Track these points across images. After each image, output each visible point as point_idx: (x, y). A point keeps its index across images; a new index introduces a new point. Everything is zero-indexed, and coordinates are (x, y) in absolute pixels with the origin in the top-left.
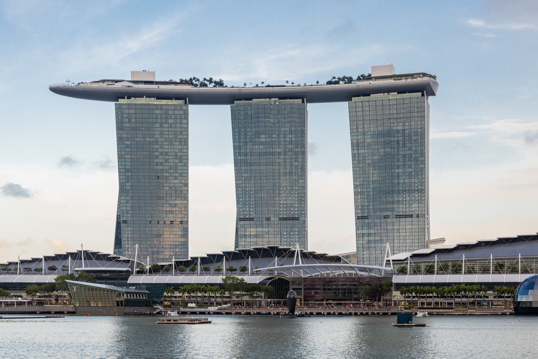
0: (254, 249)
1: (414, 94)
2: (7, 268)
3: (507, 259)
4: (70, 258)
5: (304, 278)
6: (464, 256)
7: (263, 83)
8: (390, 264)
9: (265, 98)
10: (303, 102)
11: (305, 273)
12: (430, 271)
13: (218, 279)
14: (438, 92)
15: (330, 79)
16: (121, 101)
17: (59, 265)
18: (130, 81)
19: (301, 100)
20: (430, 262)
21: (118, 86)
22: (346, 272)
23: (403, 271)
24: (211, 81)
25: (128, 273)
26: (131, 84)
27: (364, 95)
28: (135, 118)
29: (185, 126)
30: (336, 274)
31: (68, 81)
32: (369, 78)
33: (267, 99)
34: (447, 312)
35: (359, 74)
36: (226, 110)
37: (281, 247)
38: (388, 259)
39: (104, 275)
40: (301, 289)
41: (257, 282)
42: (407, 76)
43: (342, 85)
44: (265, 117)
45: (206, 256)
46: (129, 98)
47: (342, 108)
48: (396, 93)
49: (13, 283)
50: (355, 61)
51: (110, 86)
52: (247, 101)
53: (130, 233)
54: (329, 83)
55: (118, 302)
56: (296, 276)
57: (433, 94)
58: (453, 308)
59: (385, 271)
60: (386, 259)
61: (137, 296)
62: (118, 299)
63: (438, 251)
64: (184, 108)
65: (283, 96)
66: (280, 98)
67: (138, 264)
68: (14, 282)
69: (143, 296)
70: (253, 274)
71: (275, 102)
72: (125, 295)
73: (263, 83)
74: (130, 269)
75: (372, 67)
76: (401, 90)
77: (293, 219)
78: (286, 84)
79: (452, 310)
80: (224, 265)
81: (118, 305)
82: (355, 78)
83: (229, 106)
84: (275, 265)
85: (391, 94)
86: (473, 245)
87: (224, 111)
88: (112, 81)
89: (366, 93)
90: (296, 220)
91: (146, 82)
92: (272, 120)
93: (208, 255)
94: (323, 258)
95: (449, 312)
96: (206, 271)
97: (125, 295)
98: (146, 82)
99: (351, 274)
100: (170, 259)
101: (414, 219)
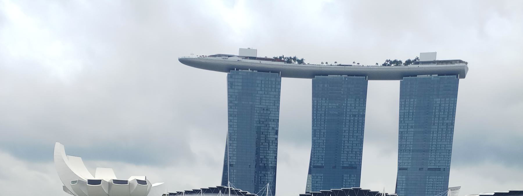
7: (336, 62)
9: (338, 75)
18: (238, 57)
24: (295, 59)
31: (192, 54)
33: (339, 76)
35: (407, 59)
47: (395, 85)
50: (405, 50)
52: (324, 77)
65: (350, 74)
71: (345, 78)
73: (336, 62)
78: (353, 65)
82: (404, 62)
83: (311, 80)
85: (433, 75)
87: (308, 83)
89: (414, 74)
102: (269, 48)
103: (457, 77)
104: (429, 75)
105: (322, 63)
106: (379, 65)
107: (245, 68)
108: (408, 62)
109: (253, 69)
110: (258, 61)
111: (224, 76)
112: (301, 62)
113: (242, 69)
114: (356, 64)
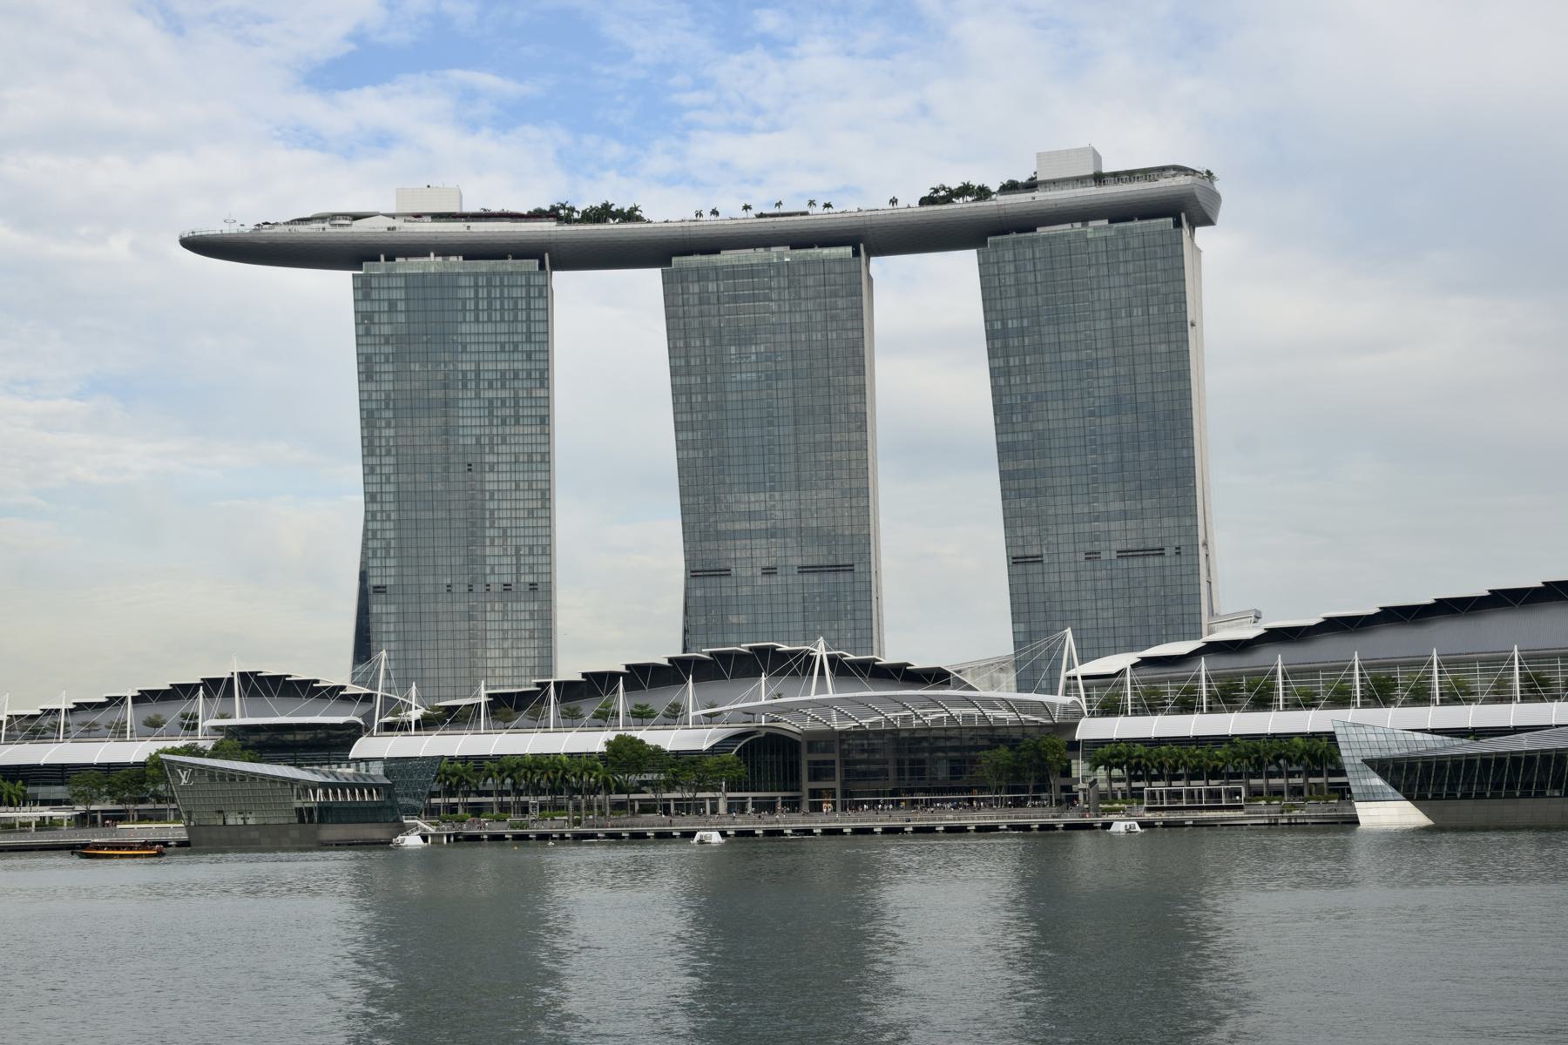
0: (711, 654)
1: (1153, 221)
2: (32, 727)
3: (1402, 665)
4: (201, 691)
5: (841, 732)
6: (1278, 660)
7: (746, 208)
8: (1077, 687)
10: (856, 253)
11: (843, 716)
12: (1186, 705)
13: (595, 741)
14: (1224, 215)
15: (927, 194)
16: (368, 268)
17: (172, 712)
18: (393, 216)
19: (849, 250)
20: (1185, 679)
21: (359, 227)
22: (955, 711)
23: (1110, 708)
25: (352, 733)
26: (397, 223)
27: (1020, 231)
28: (407, 311)
29: (540, 327)
30: (928, 719)
32: (1032, 185)
34: (1222, 819)
36: (650, 280)
37: (785, 648)
38: (1072, 673)
39: (290, 737)
40: (833, 762)
41: (705, 747)
42: (1131, 175)
43: (962, 205)
44: (755, 298)
45: (579, 678)
46: (390, 258)
48: (1105, 222)
49: (38, 766)
51: (339, 230)
52: (704, 258)
53: (392, 618)
54: (924, 201)
55: (299, 811)
56: (818, 727)
57: (1208, 221)
58: (1240, 808)
59: (1065, 707)
60: (1064, 674)
61: (335, 793)
62: (298, 804)
63: (1214, 648)
64: (539, 280)
65: (800, 240)
66: (792, 248)
67: (388, 702)
68: (42, 762)
69: (370, 793)
70: (698, 722)
72: (320, 791)
73: (746, 208)
74: (360, 721)
75: (1039, 155)
76: (1119, 213)
77: (836, 568)
79: (1239, 814)
80: (622, 701)
81: (302, 821)
84: (759, 700)
85: (1091, 224)
86: (1309, 628)
88: (344, 216)
89: (1024, 224)
90: (843, 570)
91: (437, 217)
92: (774, 306)
93: (584, 675)
94: (902, 674)
95: (1229, 819)
96: (571, 718)
97: (320, 791)
98: (437, 217)
99: (971, 716)
100: (473, 691)
101: (1167, 561)
102: (507, 179)
103: (1178, 224)
104: (1078, 225)
105: (699, 214)
106: (901, 204)
107: (417, 249)
108: (1011, 187)
109: (445, 249)
110: (458, 227)
111: (338, 284)
112: (630, 216)
113: (406, 256)
114: (818, 210)
